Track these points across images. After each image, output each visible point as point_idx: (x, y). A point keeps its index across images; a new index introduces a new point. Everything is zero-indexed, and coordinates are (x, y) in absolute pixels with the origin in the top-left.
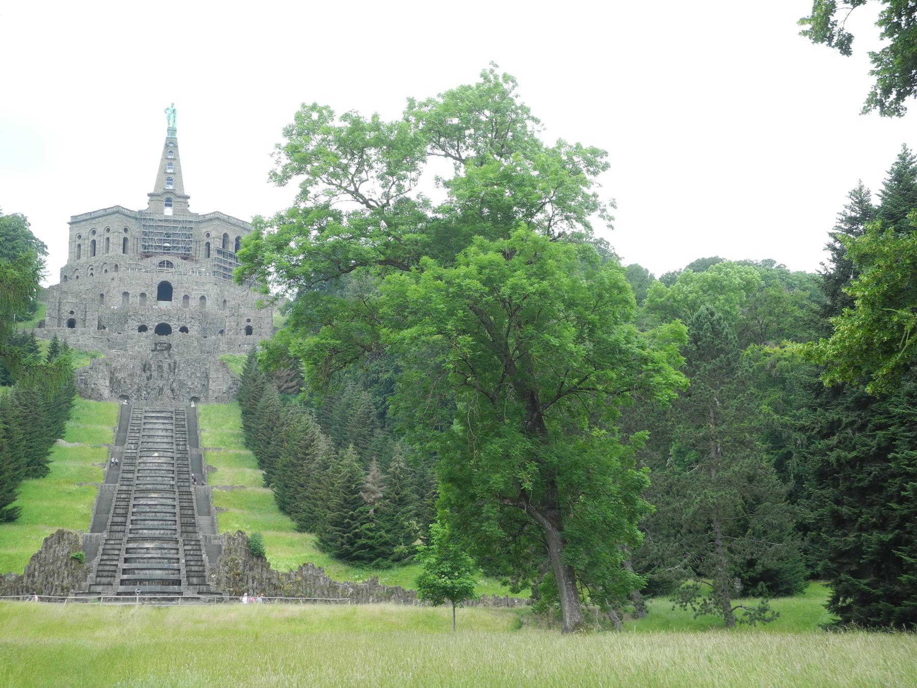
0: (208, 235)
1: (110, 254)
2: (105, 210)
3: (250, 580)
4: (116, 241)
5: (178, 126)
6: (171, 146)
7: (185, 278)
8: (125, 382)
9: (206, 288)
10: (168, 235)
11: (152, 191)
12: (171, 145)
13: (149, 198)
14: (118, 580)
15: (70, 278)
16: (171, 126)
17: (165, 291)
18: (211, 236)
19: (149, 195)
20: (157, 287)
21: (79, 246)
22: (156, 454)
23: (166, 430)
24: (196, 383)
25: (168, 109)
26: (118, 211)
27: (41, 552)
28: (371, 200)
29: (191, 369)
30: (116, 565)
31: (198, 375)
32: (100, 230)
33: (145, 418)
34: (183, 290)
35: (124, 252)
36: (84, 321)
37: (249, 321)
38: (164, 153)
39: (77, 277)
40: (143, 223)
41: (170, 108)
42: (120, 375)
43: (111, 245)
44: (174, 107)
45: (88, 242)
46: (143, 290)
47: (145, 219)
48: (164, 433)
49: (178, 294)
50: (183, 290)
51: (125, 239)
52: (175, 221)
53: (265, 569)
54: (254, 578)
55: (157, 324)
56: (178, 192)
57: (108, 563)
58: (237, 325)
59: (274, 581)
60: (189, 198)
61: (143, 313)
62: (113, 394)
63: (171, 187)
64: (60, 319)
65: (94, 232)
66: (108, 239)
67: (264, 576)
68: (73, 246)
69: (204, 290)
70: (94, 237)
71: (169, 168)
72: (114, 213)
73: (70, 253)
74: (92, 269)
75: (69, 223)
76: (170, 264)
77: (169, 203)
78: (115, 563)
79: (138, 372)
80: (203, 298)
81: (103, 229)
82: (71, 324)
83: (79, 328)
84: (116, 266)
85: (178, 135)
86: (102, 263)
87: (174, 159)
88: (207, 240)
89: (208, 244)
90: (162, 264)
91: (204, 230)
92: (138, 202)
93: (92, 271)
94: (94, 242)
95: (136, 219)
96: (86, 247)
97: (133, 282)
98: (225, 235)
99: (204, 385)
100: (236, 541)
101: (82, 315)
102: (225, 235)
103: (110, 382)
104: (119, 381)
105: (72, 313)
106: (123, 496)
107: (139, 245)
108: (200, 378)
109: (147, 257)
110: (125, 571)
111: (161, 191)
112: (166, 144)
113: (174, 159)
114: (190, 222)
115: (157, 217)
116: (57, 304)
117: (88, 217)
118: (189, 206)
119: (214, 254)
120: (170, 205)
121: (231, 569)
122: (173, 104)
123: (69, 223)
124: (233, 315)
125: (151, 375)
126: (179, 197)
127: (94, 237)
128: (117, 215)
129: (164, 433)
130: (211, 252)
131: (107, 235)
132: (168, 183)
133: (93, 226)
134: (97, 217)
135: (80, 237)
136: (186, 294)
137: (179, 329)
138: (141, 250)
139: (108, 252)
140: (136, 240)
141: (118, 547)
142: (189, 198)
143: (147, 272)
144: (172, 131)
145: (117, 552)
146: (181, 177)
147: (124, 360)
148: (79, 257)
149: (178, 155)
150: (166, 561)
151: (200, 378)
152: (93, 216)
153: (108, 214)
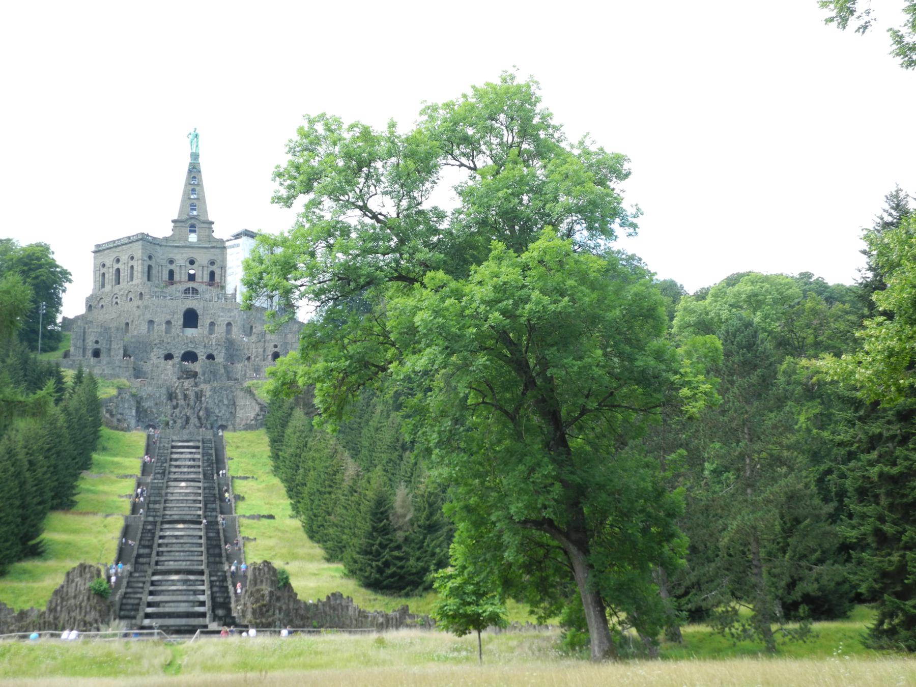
1: (135, 282)
2: (129, 238)
3: (277, 612)
4: (139, 267)
6: (194, 172)
7: (211, 304)
9: (232, 314)
11: (176, 217)
13: (173, 224)
14: (141, 614)
15: (95, 308)
16: (194, 151)
17: (191, 319)
19: (173, 221)
20: (182, 314)
21: (104, 274)
22: (183, 484)
23: (194, 460)
25: (190, 134)
26: (144, 239)
27: (62, 587)
28: (381, 214)
29: (218, 397)
30: (141, 599)
31: (226, 402)
32: (124, 258)
33: (173, 447)
35: (149, 280)
36: (109, 350)
38: (188, 178)
39: (102, 306)
41: (193, 132)
42: (146, 404)
43: (135, 273)
45: (112, 271)
46: (168, 317)
48: (192, 463)
49: (204, 321)
51: (150, 267)
53: (292, 600)
54: (280, 609)
55: (183, 352)
56: (202, 218)
57: (132, 596)
58: (264, 351)
59: (302, 612)
60: (213, 223)
61: (169, 341)
62: (140, 423)
63: (195, 213)
64: (84, 350)
65: (118, 261)
66: (132, 267)
67: (291, 606)
68: (98, 275)
69: (230, 317)
70: (120, 266)
71: (193, 194)
72: (138, 240)
73: (95, 282)
74: (117, 298)
75: (94, 252)
76: (195, 291)
77: (193, 228)
78: (139, 596)
80: (229, 324)
81: (126, 257)
82: (96, 354)
83: (104, 358)
84: (141, 294)
85: (200, 160)
86: (127, 292)
87: (198, 185)
90: (187, 291)
92: (162, 230)
93: (116, 300)
94: (118, 270)
96: (110, 276)
99: (231, 413)
100: (262, 571)
101: (107, 344)
103: (137, 411)
104: (146, 411)
105: (97, 342)
106: (149, 527)
108: (228, 406)
110: (150, 605)
111: (185, 217)
113: (198, 185)
118: (213, 231)
120: (195, 231)
121: (257, 601)
122: (196, 129)
123: (94, 252)
125: (177, 404)
126: (204, 223)
127: (120, 266)
128: (140, 242)
129: (192, 463)
131: (131, 263)
132: (192, 209)
134: (124, 245)
135: (104, 265)
137: (205, 356)
139: (132, 279)
141: (143, 579)
142: (213, 223)
143: (172, 299)
144: (195, 156)
145: (141, 585)
146: (205, 202)
147: (150, 389)
148: (103, 286)
149: (201, 180)
150: (192, 593)
151: (228, 406)
152: (117, 244)
153: (132, 242)
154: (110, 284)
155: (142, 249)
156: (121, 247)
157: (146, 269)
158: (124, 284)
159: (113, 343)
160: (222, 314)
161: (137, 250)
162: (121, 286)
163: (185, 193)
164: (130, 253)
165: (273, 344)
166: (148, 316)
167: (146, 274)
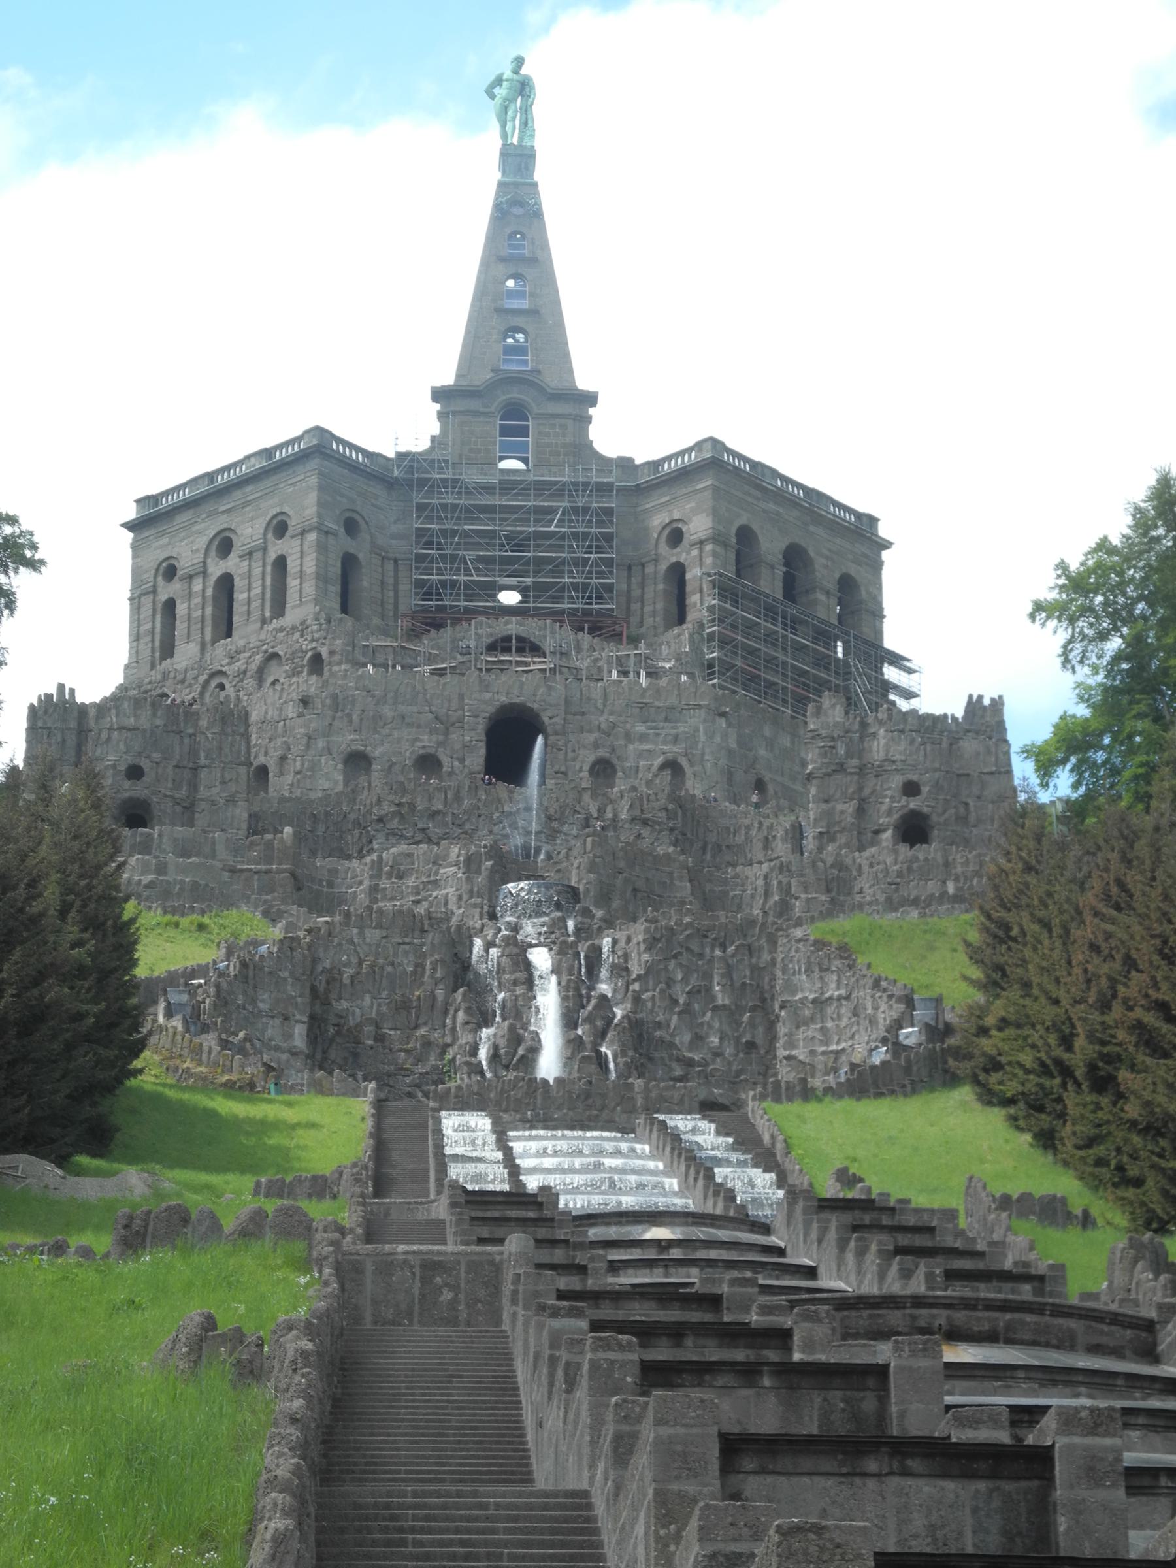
0: (676, 537)
1: (292, 616)
5: (542, 144)
8: (380, 1038)
9: (682, 729)
11: (448, 378)
12: (518, 211)
18: (688, 538)
20: (481, 728)
21: (170, 605)
24: (715, 1040)
25: (499, 81)
34: (590, 738)
35: (344, 609)
37: (911, 789)
40: (417, 498)
41: (508, 74)
44: (524, 71)
46: (428, 742)
47: (422, 482)
50: (590, 738)
51: (349, 563)
52: (541, 488)
56: (552, 381)
58: (861, 811)
60: (591, 399)
66: (281, 563)
68: (146, 610)
69: (676, 740)
70: (232, 564)
73: (136, 637)
75: (130, 526)
79: (440, 994)
81: (259, 526)
85: (542, 174)
86: (259, 658)
88: (670, 556)
89: (678, 572)
91: (658, 521)
94: (226, 584)
95: (390, 484)
97: (387, 711)
98: (745, 535)
99: (751, 1045)
102: (745, 535)
105: (135, 773)
107: (404, 587)
108: (732, 1013)
109: (438, 626)
111: (484, 376)
112: (497, 207)
114: (604, 489)
115: (472, 476)
116: (72, 740)
117: (204, 488)
120: (524, 432)
123: (130, 526)
124: (841, 768)
127: (232, 564)
130: (693, 599)
131: (276, 549)
133: (221, 522)
135: (170, 572)
136: (602, 753)
138: (410, 601)
139: (279, 608)
140: (390, 566)
143: (440, 673)
147: (372, 935)
148: (168, 649)
149: (545, 246)
154: (196, 636)
155: (321, 488)
156: (238, 494)
157: (336, 569)
158: (247, 632)
159: (203, 774)
160: (640, 728)
162: (238, 639)
165: (896, 781)
166: (347, 740)
167: (335, 589)
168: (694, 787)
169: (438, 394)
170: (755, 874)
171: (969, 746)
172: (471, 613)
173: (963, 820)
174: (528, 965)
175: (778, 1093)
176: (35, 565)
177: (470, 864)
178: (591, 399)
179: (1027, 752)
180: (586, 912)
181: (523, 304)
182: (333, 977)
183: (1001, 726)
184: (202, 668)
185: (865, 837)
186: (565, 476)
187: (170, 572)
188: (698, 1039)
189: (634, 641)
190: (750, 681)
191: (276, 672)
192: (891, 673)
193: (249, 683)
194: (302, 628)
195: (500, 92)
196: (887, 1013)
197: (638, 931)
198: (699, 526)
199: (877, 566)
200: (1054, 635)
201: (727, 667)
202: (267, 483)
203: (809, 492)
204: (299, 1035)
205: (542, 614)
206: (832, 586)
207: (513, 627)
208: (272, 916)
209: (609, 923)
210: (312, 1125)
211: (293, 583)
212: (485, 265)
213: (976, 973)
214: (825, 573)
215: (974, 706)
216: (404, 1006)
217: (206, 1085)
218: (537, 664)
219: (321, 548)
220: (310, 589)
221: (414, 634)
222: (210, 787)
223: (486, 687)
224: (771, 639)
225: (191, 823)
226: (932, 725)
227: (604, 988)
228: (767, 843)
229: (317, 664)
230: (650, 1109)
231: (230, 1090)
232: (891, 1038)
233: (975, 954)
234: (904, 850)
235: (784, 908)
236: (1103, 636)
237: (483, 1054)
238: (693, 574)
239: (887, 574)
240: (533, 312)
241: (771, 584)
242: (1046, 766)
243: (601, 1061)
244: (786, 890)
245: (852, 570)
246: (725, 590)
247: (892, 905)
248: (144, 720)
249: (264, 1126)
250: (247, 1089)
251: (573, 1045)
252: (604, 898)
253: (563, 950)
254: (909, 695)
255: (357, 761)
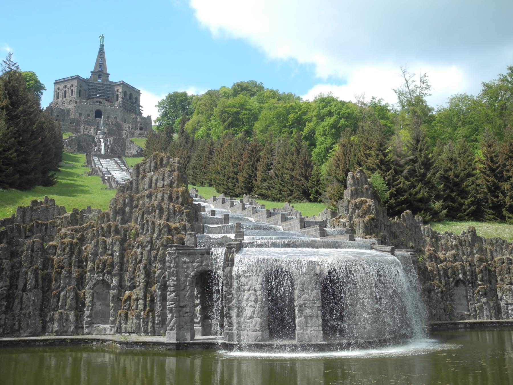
0: (118, 91)
1: (73, 96)
2: (71, 77)
6: (101, 53)
10: (100, 90)
21: (59, 93)
26: (78, 78)
32: (69, 86)
38: (98, 55)
46: (88, 112)
51: (80, 91)
52: (103, 84)
56: (105, 72)
58: (136, 126)
60: (109, 74)
66: (72, 90)
70: (66, 89)
75: (54, 83)
80: (116, 118)
85: (105, 47)
89: (118, 95)
91: (116, 89)
92: (86, 75)
94: (65, 91)
95: (85, 82)
96: (61, 94)
98: (125, 92)
102: (125, 92)
105: (58, 116)
109: (90, 99)
119: (120, 99)
120: (101, 77)
122: (103, 34)
123: (54, 83)
127: (66, 89)
130: (119, 98)
131: (72, 88)
133: (65, 84)
135: (59, 89)
139: (72, 95)
144: (102, 46)
147: (84, 137)
148: (58, 98)
158: (68, 97)
161: (75, 83)
162: (67, 98)
163: (97, 61)
164: (71, 83)
166: (80, 112)
168: (118, 120)
169: (91, 72)
170: (125, 132)
171: (147, 120)
172: (94, 98)
173: (146, 128)
174: (101, 141)
175: (126, 157)
176: (45, 90)
177: (94, 129)
178: (109, 74)
179: (154, 121)
180: (106, 135)
181: (102, 63)
182: (80, 141)
183: (151, 119)
184: (62, 101)
185: (136, 129)
186: (105, 83)
187: (59, 89)
188: (118, 150)
189: (112, 102)
190: (125, 108)
191: (71, 102)
192: (140, 108)
193: (68, 103)
194: (75, 98)
195: (101, 37)
196: (137, 149)
197: (112, 138)
198: (120, 90)
199: (140, 96)
200: (157, 109)
201: (122, 107)
202: (71, 81)
203: (133, 87)
204: (77, 147)
205: (102, 98)
206: (135, 98)
207: (98, 100)
208: (73, 133)
209: (109, 137)
210: (80, 157)
211: (74, 92)
212: (98, 57)
213: (145, 146)
214: (134, 96)
215: (148, 116)
216: (87, 144)
217: (68, 152)
218: (101, 105)
219: (77, 89)
220: (76, 93)
221: (87, 100)
222: (66, 118)
223: (95, 107)
224: (127, 104)
225: (64, 122)
226: (144, 118)
227: (108, 144)
228: (126, 127)
229: (76, 102)
230: (113, 157)
231: (71, 153)
232: (137, 152)
233: (145, 144)
234: (140, 131)
235: (127, 136)
236: (162, 109)
237: (96, 150)
238: (119, 96)
239: (141, 97)
240: (103, 64)
241: (128, 98)
242: (155, 123)
243: (108, 151)
244: (127, 134)
245: (137, 96)
246: (123, 98)
247: (138, 137)
248: (59, 110)
249: (76, 157)
250: (72, 153)
251: (105, 149)
252: (108, 134)
253: (104, 140)
254: (142, 110)
255: (80, 114)
